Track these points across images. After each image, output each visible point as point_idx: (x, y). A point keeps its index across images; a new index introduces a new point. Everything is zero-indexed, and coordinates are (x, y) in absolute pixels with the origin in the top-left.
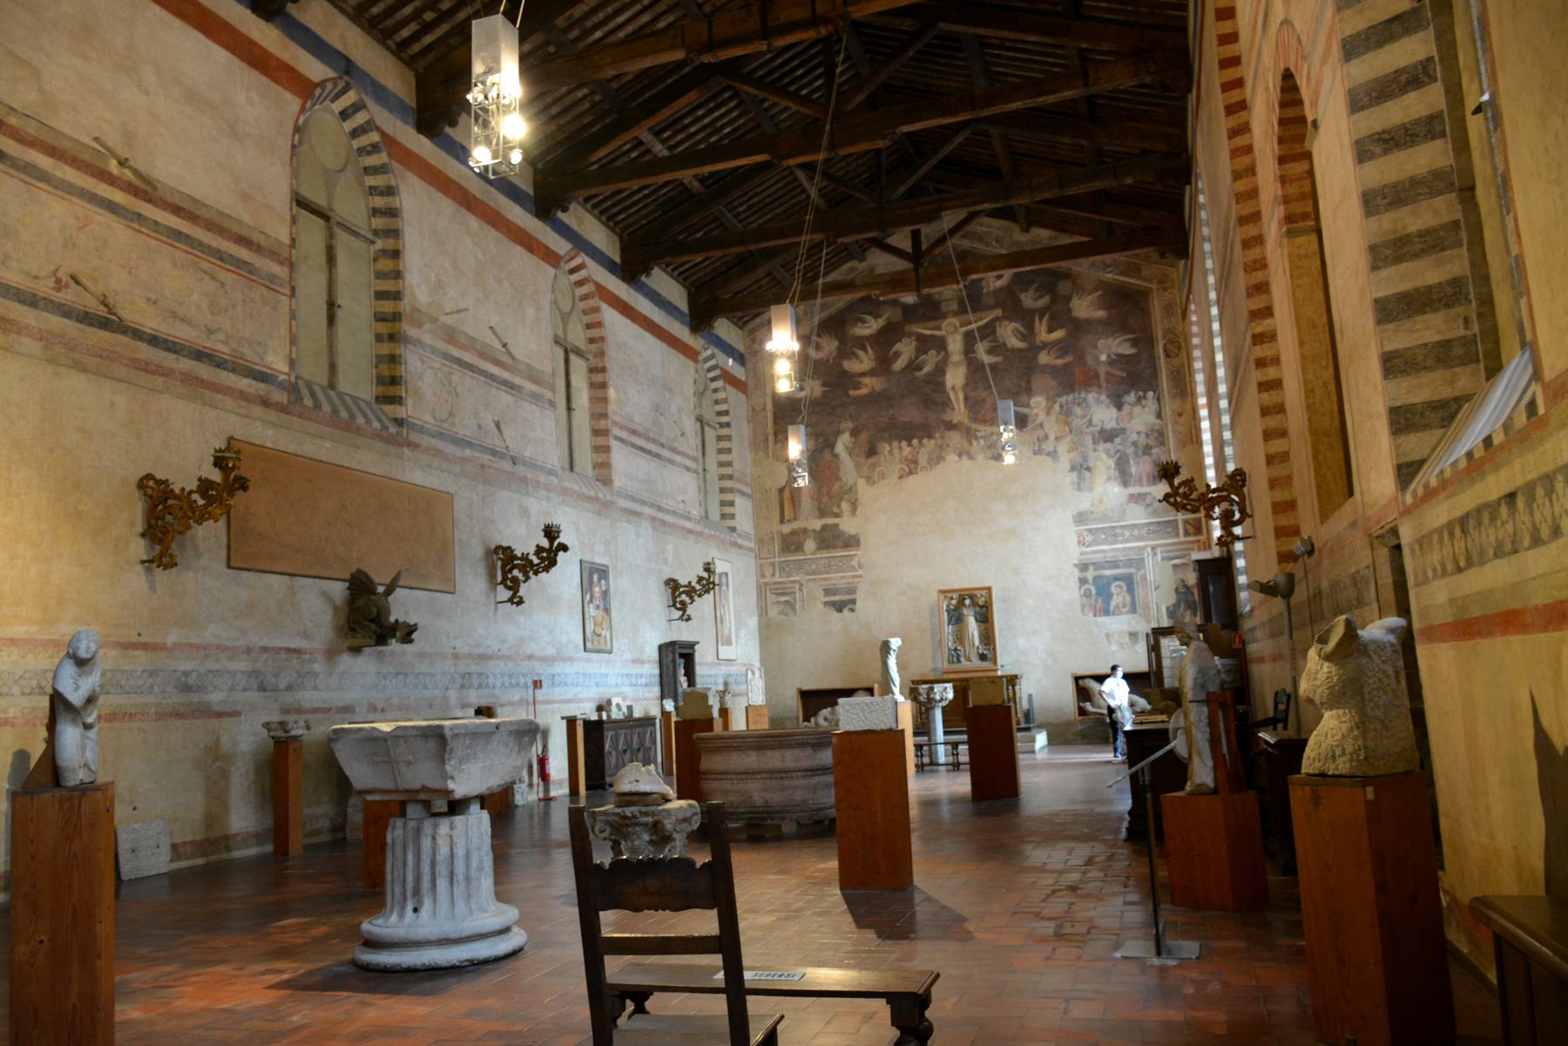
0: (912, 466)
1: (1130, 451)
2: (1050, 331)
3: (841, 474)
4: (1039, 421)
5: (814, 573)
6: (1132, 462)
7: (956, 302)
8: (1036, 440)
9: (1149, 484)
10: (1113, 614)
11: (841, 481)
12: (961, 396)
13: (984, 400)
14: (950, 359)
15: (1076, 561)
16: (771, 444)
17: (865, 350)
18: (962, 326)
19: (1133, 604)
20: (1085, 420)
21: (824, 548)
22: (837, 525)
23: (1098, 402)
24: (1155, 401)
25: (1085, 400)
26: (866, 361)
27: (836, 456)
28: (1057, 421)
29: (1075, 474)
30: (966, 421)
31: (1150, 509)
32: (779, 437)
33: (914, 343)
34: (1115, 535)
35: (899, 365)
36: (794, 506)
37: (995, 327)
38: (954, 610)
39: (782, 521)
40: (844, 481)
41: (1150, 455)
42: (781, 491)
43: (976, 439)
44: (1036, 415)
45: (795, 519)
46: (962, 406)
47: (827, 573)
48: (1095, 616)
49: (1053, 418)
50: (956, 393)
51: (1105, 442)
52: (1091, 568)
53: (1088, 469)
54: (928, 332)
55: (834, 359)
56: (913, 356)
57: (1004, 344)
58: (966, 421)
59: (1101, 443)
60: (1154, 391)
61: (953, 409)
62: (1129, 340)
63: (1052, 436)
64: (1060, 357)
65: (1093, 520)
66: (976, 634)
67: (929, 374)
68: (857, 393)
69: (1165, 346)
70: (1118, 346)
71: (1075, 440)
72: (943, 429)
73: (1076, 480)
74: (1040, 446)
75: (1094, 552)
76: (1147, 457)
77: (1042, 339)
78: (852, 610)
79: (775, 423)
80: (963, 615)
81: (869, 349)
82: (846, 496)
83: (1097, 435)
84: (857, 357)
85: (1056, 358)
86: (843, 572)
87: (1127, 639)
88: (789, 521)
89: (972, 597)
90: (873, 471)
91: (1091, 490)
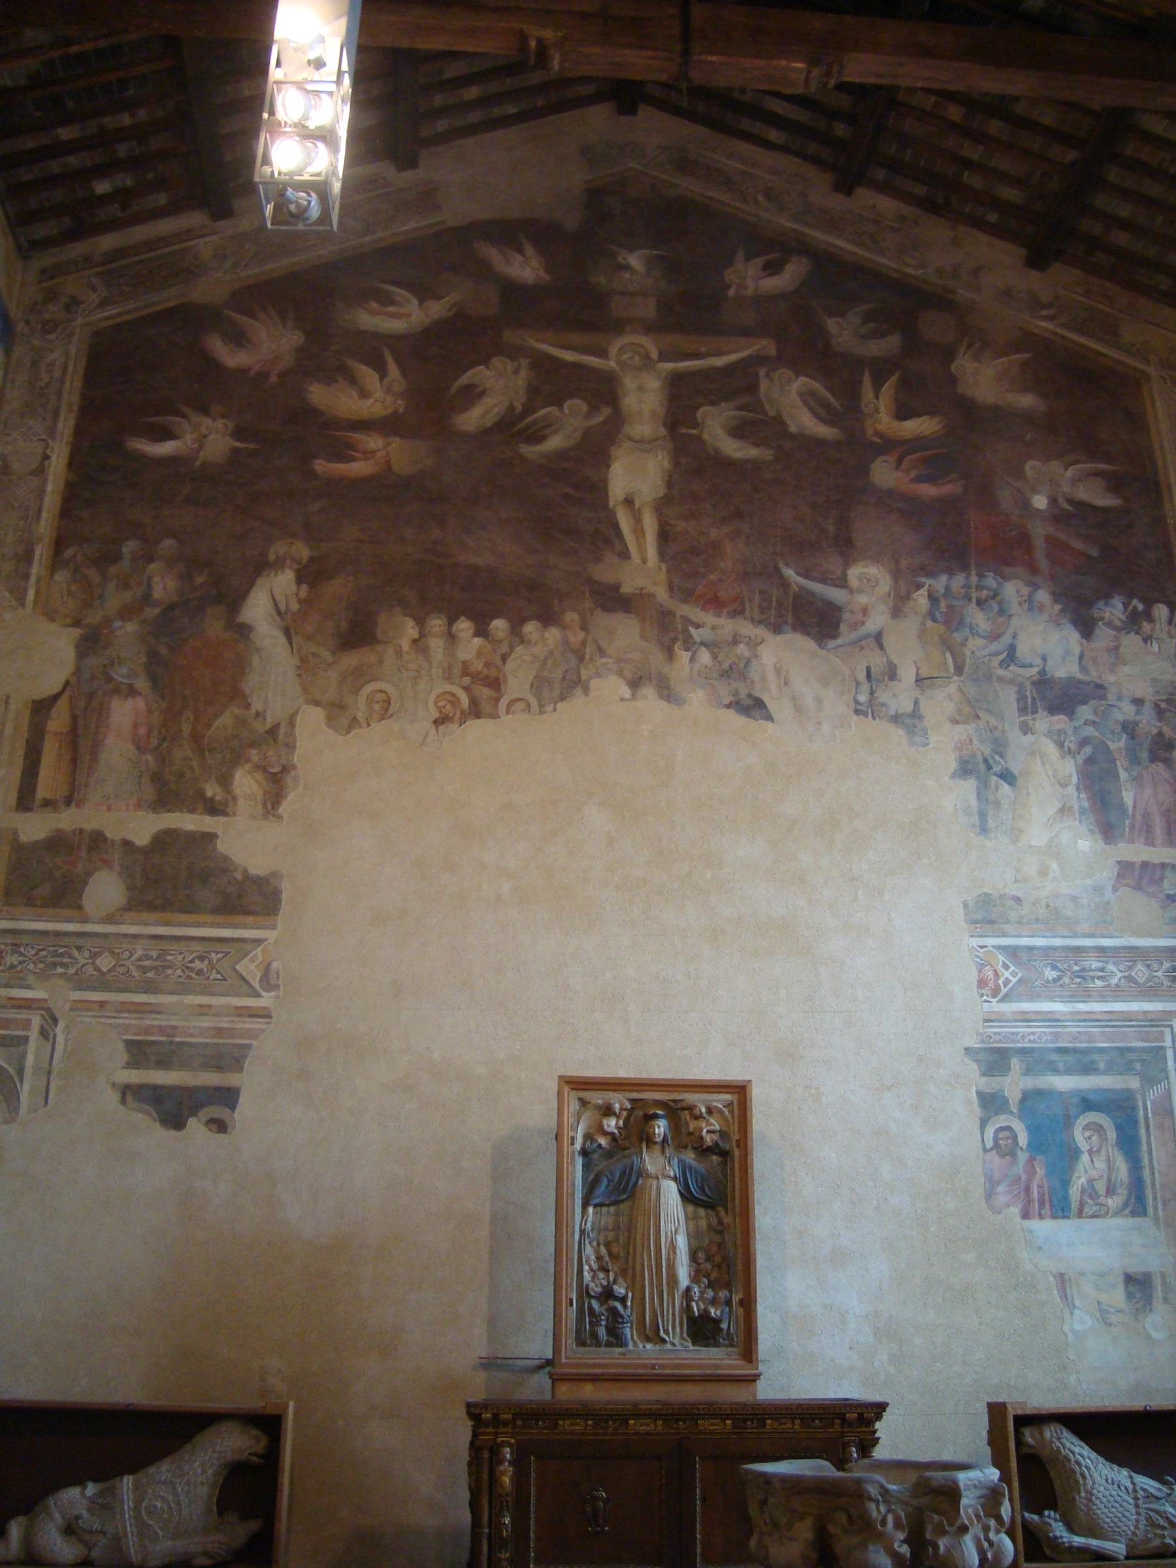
0: (484, 692)
1: (1118, 745)
2: (903, 413)
3: (250, 683)
5: (103, 982)
6: (1123, 775)
7: (652, 301)
8: (861, 676)
10: (1080, 1214)
11: (248, 706)
12: (650, 524)
13: (716, 546)
14: (627, 429)
15: (972, 1042)
16: (36, 569)
17: (382, 371)
18: (664, 357)
19: (1137, 1185)
20: (995, 646)
21: (152, 907)
22: (211, 837)
23: (1030, 604)
25: (995, 595)
26: (379, 394)
27: (244, 631)
28: (922, 635)
29: (969, 785)
30: (661, 594)
32: (69, 552)
33: (524, 372)
34: (1082, 974)
35: (473, 418)
36: (74, 761)
37: (756, 376)
38: (609, 1154)
39: (25, 801)
40: (257, 705)
42: (41, 708)
43: (689, 643)
44: (865, 611)
45: (68, 801)
46: (652, 552)
47: (149, 988)
48: (1026, 1215)
49: (910, 626)
50: (637, 518)
51: (1053, 710)
52: (1015, 1063)
53: (1008, 777)
54: (569, 356)
55: (282, 375)
56: (519, 409)
57: (779, 421)
58: (661, 594)
59: (1042, 713)
61: (624, 555)
62: (1096, 474)
63: (908, 674)
64: (930, 479)
66: (682, 1242)
67: (561, 455)
68: (339, 468)
70: (1074, 481)
71: (972, 691)
72: (588, 604)
73: (974, 802)
74: (872, 693)
76: (1160, 767)
77: (879, 427)
78: (220, 1126)
79: (65, 512)
80: (642, 1173)
81: (394, 371)
82: (254, 754)
83: (1028, 687)
84: (353, 380)
85: (918, 480)
86: (203, 992)
87: (1118, 1296)
88: (48, 803)
89: (674, 1111)
90: (356, 691)
91: (1016, 834)
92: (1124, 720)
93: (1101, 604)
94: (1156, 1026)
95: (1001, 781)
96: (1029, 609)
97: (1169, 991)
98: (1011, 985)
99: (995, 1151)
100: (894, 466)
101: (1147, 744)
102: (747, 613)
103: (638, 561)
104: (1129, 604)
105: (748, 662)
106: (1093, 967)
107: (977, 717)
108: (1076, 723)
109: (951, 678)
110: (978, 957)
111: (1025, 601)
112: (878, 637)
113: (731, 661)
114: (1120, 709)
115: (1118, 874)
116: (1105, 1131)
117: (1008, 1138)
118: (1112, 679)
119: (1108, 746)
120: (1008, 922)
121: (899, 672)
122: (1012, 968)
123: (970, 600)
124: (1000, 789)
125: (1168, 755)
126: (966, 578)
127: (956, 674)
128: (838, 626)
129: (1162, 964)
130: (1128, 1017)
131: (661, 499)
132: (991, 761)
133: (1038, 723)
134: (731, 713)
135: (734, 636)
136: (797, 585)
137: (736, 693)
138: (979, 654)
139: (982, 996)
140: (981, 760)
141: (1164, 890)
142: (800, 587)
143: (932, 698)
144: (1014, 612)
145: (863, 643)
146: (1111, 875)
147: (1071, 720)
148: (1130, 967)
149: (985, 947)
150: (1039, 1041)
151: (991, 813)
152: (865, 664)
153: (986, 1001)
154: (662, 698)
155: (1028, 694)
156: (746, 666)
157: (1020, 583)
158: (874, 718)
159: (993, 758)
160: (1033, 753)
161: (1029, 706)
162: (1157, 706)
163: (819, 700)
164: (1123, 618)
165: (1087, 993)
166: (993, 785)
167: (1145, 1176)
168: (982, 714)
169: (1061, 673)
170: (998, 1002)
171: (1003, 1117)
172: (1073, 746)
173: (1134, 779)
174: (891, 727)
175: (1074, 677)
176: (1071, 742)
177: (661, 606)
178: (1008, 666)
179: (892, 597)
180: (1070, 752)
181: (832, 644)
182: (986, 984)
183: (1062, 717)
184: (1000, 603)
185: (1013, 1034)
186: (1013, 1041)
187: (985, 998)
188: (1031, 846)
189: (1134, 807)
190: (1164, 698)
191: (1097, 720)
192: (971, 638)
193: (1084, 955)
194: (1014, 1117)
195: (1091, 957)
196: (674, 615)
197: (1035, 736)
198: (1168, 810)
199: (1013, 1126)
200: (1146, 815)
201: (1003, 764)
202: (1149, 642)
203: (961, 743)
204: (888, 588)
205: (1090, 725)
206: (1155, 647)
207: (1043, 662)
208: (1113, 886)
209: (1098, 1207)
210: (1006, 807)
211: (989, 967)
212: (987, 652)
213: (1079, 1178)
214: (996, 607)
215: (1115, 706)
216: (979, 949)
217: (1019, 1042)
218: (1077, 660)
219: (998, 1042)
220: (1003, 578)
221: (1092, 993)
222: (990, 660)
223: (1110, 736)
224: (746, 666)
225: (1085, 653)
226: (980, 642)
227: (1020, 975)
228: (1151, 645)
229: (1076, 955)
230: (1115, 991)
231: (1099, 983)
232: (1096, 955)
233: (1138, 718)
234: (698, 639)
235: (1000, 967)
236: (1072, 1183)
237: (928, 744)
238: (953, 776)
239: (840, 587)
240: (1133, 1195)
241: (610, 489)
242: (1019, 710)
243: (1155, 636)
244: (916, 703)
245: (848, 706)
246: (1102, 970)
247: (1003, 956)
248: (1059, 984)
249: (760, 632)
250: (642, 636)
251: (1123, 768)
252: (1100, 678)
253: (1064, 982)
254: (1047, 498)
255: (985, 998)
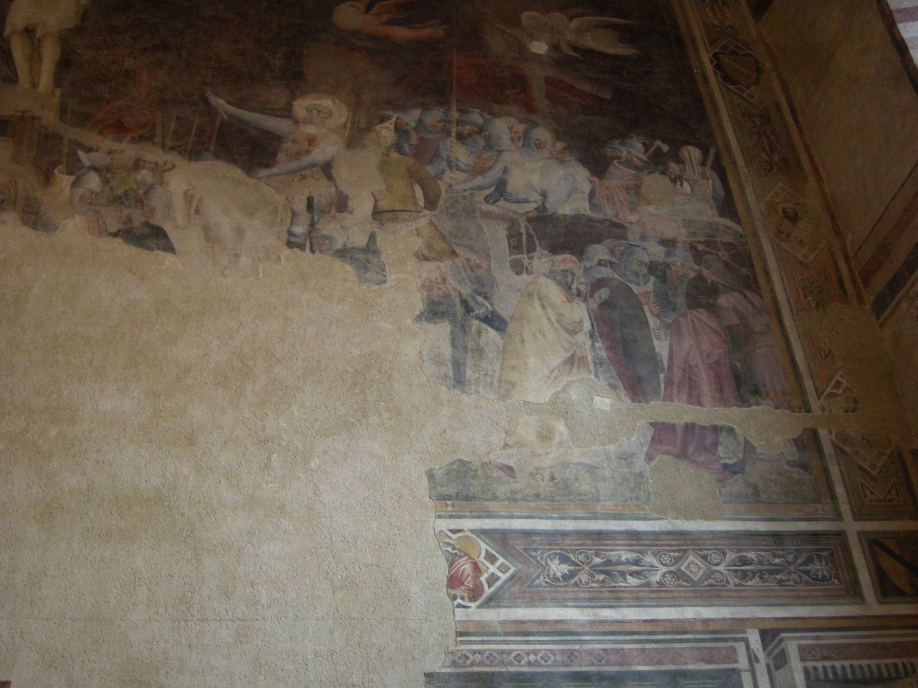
1: (645, 288)
4: (318, 155)
6: (653, 322)
8: (300, 205)
9: (724, 402)
12: (50, 53)
20: (479, 181)
23: (525, 141)
24: (709, 172)
25: (480, 131)
28: (384, 166)
29: (441, 331)
30: (49, 118)
31: (736, 485)
34: (607, 569)
41: (712, 309)
43: (74, 167)
44: (312, 141)
46: (46, 78)
51: (554, 250)
53: (495, 321)
58: (49, 118)
60: (705, 150)
62: (607, 26)
63: (363, 206)
65: (512, 498)
69: (715, 55)
71: (447, 226)
73: (447, 350)
74: (312, 225)
75: (521, 630)
76: (702, 315)
83: (523, 224)
85: (391, 23)
91: (506, 388)
92: (651, 262)
93: (616, 143)
94: (726, 640)
95: (484, 326)
96: (524, 145)
97: (736, 591)
98: (499, 583)
100: (363, 10)
101: (683, 288)
102: (158, 139)
103: (27, 86)
104: (653, 144)
105: (150, 188)
106: (623, 558)
107: (454, 254)
108: (588, 264)
109: (420, 212)
110: (449, 544)
111: (519, 138)
112: (327, 169)
113: (127, 187)
114: (644, 249)
115: (653, 439)
118: (633, 218)
119: (630, 289)
120: (494, 498)
121: (351, 204)
122: (501, 560)
123: (449, 134)
124: (483, 335)
125: (711, 301)
126: (444, 113)
127: (425, 208)
128: (274, 154)
129: (724, 554)
130: (679, 628)
131: (70, 30)
132: (471, 303)
133: (535, 262)
134: (119, 240)
135: (137, 161)
136: (226, 113)
137: (129, 220)
138: (460, 188)
139: (454, 598)
140: (457, 301)
141: (720, 458)
142: (231, 116)
143: (393, 232)
144: (504, 148)
145: (307, 172)
146: (643, 440)
147: (580, 260)
148: (677, 560)
149: (460, 531)
150: (543, 663)
151: (470, 362)
152: (307, 194)
153: (459, 606)
154: (25, 222)
155: (523, 230)
156: (146, 193)
157: (513, 121)
158: (313, 251)
159: (475, 299)
160: (530, 295)
161: (525, 244)
162: (693, 248)
163: (239, 231)
164: (645, 158)
165: (616, 595)
166: (473, 329)
168: (457, 250)
169: (567, 210)
170: (478, 607)
172: (583, 288)
173: (669, 326)
174: (337, 263)
175: (583, 215)
176: (582, 283)
177: (46, 129)
178: (495, 202)
179: (348, 130)
180: (579, 294)
181: (264, 173)
182: (462, 584)
183: (568, 256)
184: (488, 138)
185: (502, 652)
186: (502, 663)
187: (459, 601)
188: (526, 403)
189: (671, 358)
190: (701, 239)
191: (614, 260)
192: (448, 172)
193: (608, 542)
195: (618, 545)
196: (61, 138)
197: (533, 276)
198: (717, 363)
200: (689, 370)
201: (488, 306)
202: (679, 183)
203: (431, 282)
204: (344, 120)
205: (606, 266)
206: (687, 187)
207: (543, 198)
208: (647, 454)
210: (491, 355)
211: (465, 558)
212: (466, 186)
214: (482, 143)
215: (639, 246)
216: (450, 534)
217: (511, 664)
218: (586, 196)
219: (481, 664)
220: (489, 113)
221: (620, 595)
222: (471, 194)
223: (632, 278)
224: (146, 193)
225: (598, 191)
226: (461, 176)
227: (513, 569)
228: (681, 185)
229: (597, 542)
230: (657, 591)
231: (632, 581)
232: (627, 542)
233: (669, 260)
234: (87, 163)
235: (482, 558)
237: (385, 282)
238: (419, 318)
239: (281, 117)
241: (8, 19)
242: (511, 247)
243: (685, 176)
244: (372, 237)
245: (279, 238)
246: (637, 562)
247: (487, 544)
248: (573, 581)
249: (171, 158)
250: (13, 159)
251: (652, 312)
252: (616, 217)
253: (580, 580)
254: (548, 44)
255: (459, 601)
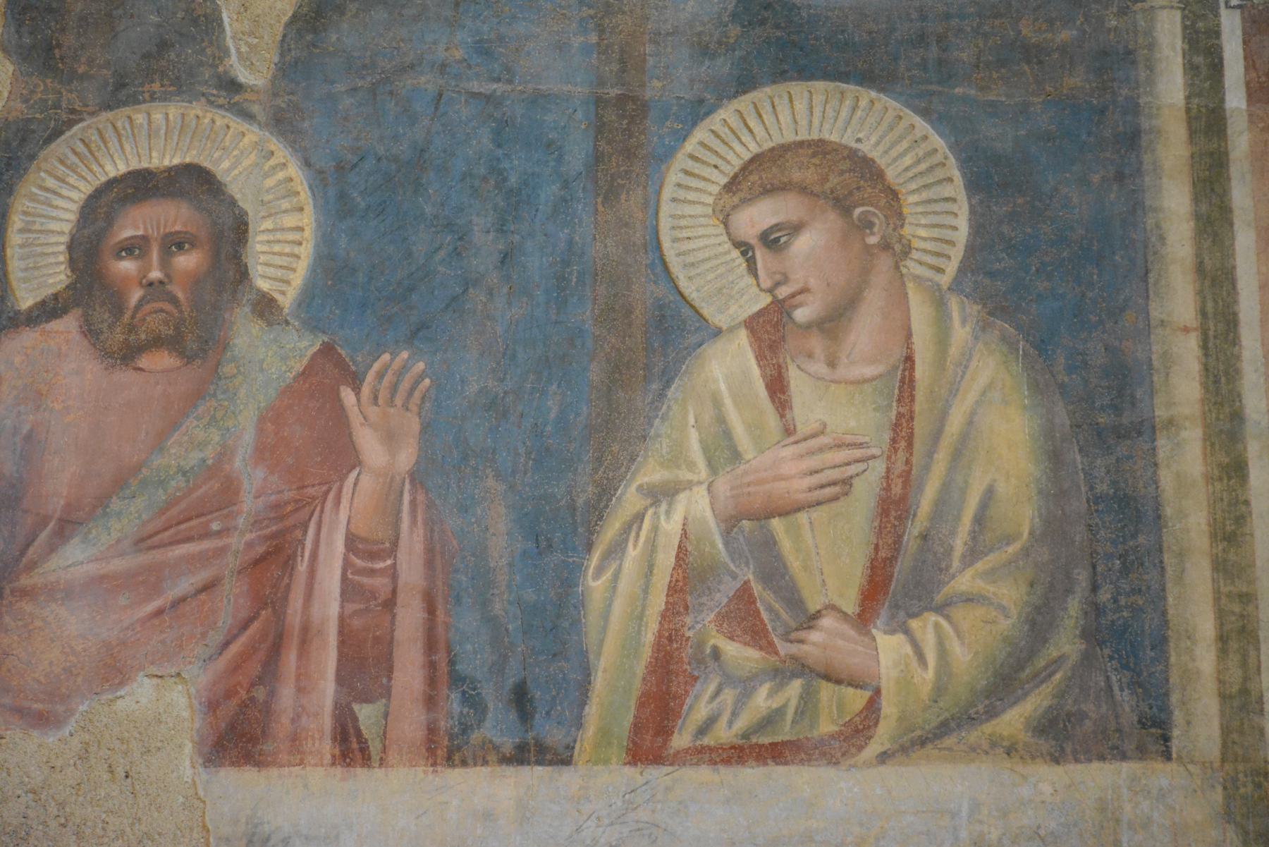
99: (68, 325)
116: (894, 194)
117: (176, 243)
167: (1166, 478)
171: (167, 114)
194: (249, 116)
199: (222, 168)
209: (796, 686)
213: (662, 494)
236: (610, 531)
240: (1074, 606)
